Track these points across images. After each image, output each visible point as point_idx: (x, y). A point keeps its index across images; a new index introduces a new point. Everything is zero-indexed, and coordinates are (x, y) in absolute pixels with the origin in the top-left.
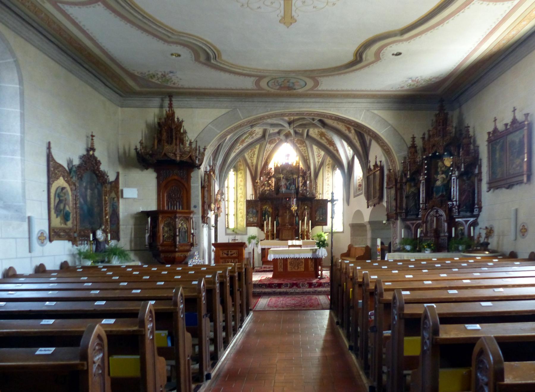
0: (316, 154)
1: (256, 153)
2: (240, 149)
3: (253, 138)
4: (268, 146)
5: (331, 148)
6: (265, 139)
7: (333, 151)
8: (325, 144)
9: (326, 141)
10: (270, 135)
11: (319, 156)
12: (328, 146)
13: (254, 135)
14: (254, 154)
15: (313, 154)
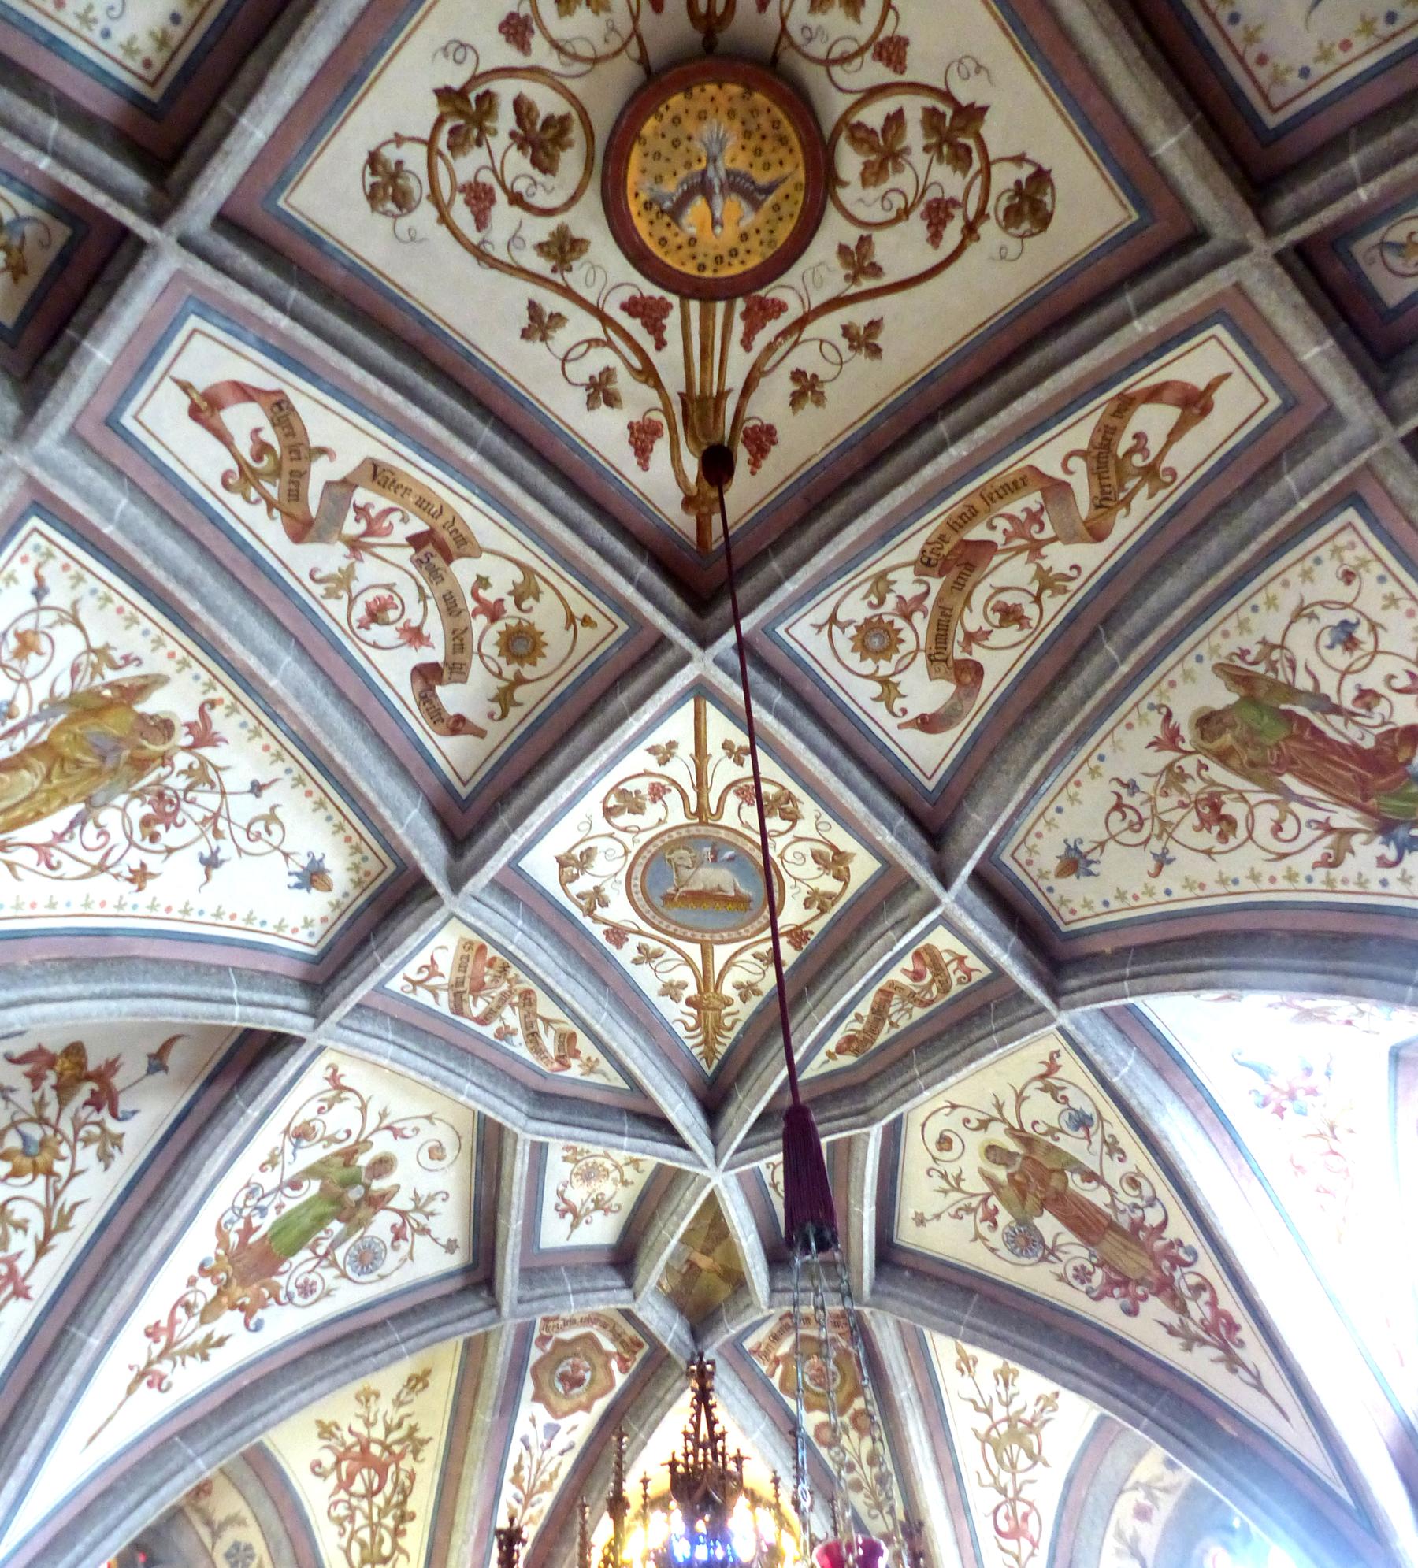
0: (982, 1500)
1: (422, 1502)
2: (222, 1362)
3: (367, 1260)
4: (530, 1414)
5: (1148, 1328)
6: (495, 1305)
7: (1169, 1350)
8: (1075, 1299)
9: (1076, 1252)
10: (542, 1269)
11: (1015, 1533)
12: (1108, 1313)
13: (382, 1224)
14: (404, 1517)
15: (959, 1506)
